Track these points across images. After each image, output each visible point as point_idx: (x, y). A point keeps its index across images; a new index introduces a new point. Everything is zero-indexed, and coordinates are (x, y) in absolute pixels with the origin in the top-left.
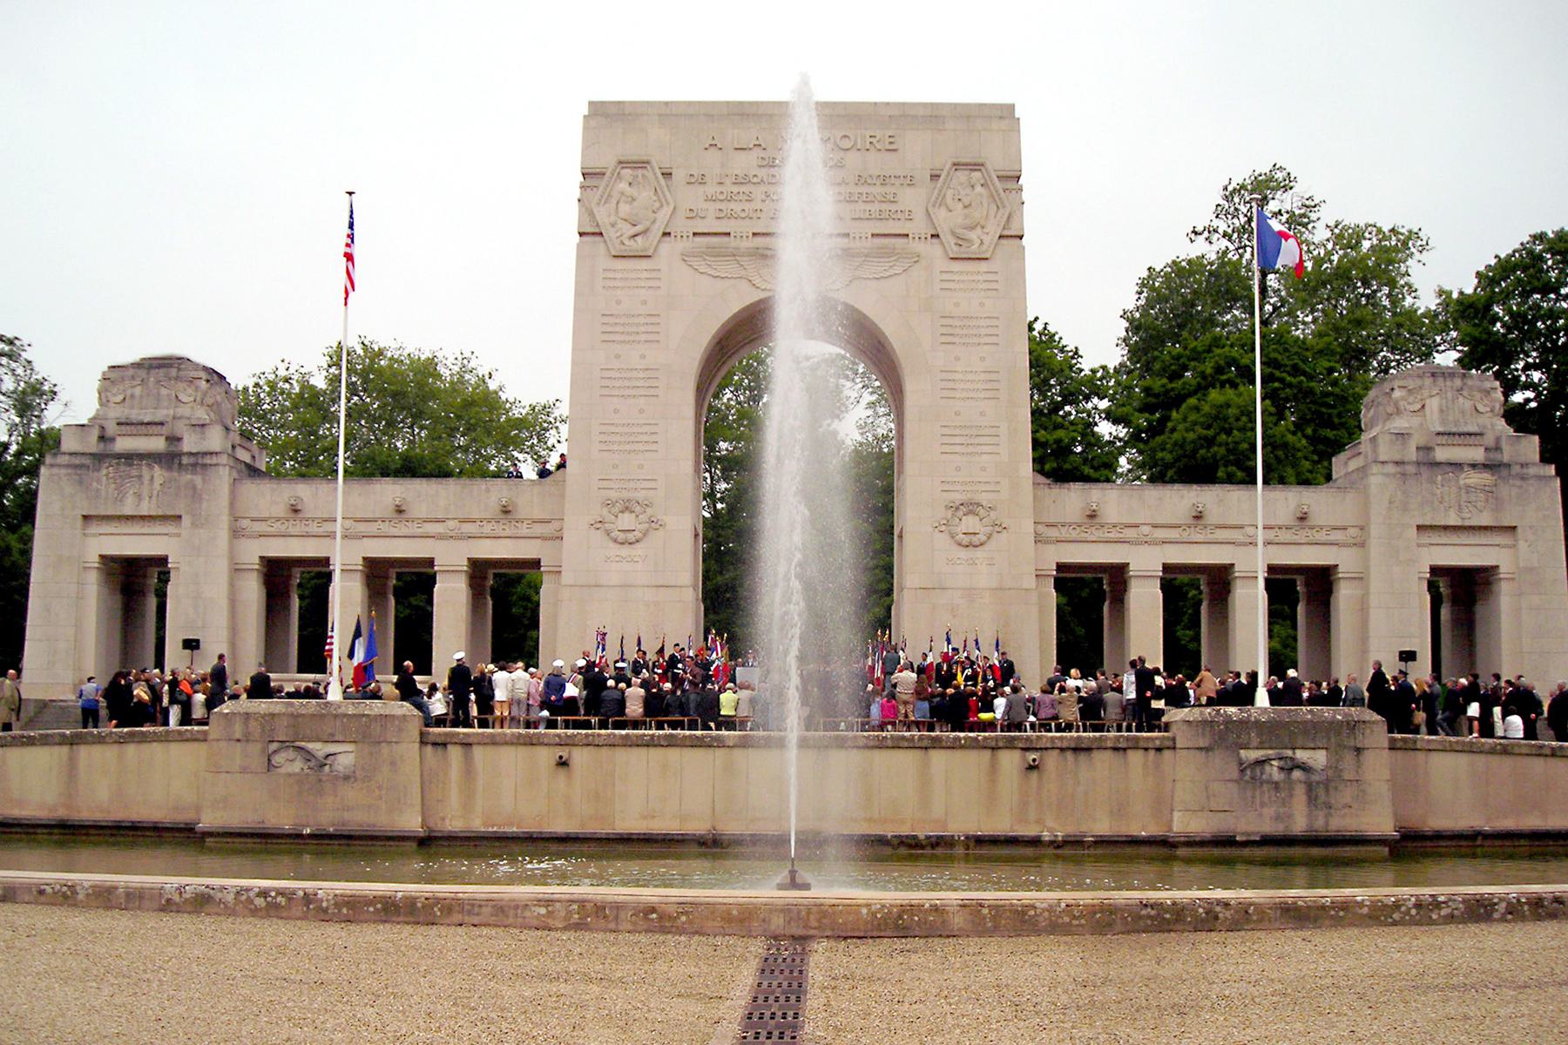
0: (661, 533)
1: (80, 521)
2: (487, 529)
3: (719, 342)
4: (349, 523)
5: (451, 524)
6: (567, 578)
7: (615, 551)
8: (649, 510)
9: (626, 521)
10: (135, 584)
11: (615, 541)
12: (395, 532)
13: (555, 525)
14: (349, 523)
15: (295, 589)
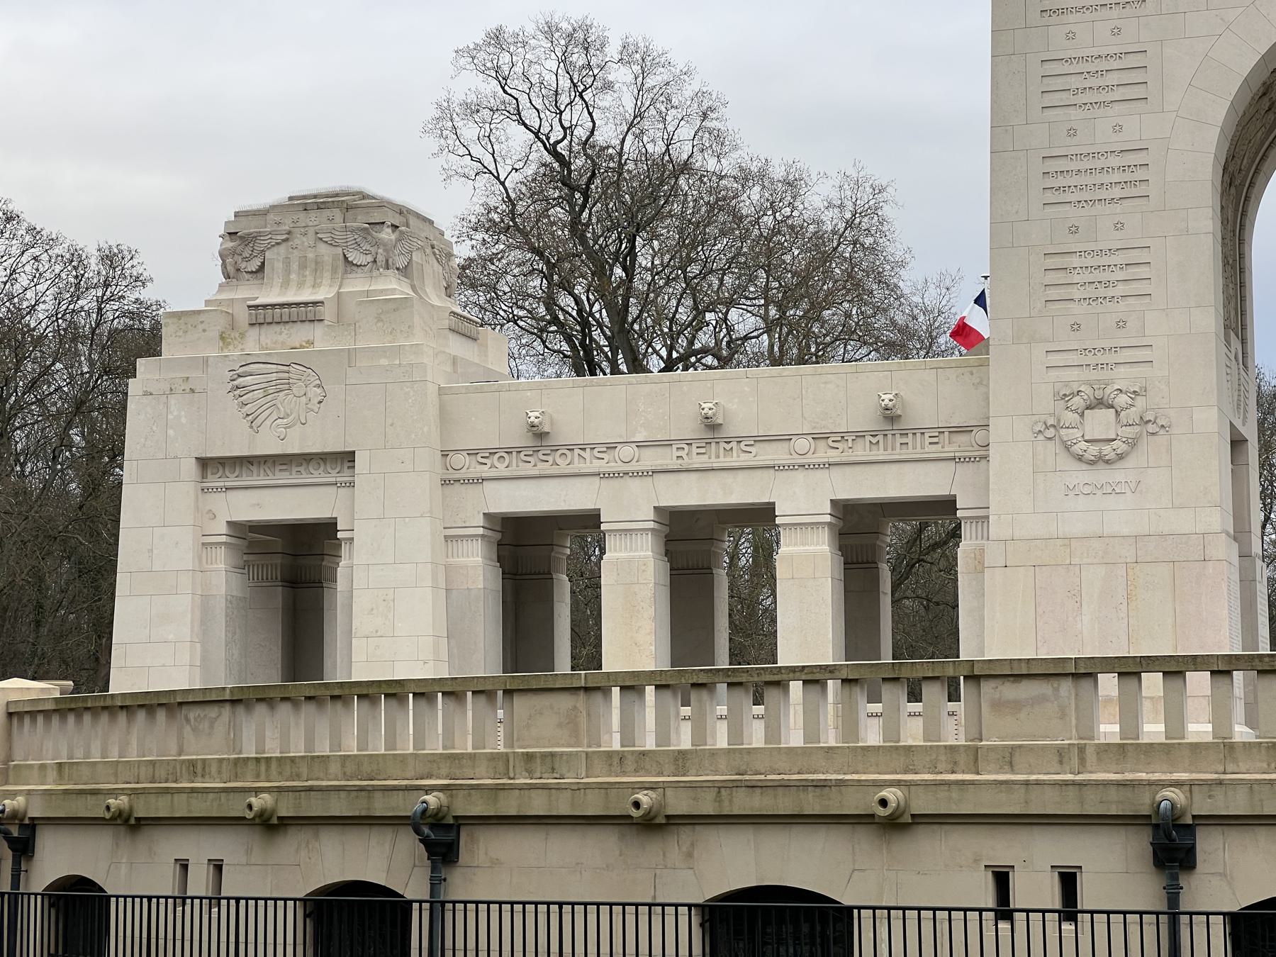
0: (1162, 439)
1: (190, 468)
2: (861, 451)
3: (1266, 90)
4: (631, 448)
5: (627, 452)
6: (996, 528)
7: (1081, 476)
8: (1140, 402)
9: (1100, 423)
10: (293, 569)
11: (1080, 458)
12: (529, 470)
13: (979, 436)
14: (631, 448)
15: (537, 562)
